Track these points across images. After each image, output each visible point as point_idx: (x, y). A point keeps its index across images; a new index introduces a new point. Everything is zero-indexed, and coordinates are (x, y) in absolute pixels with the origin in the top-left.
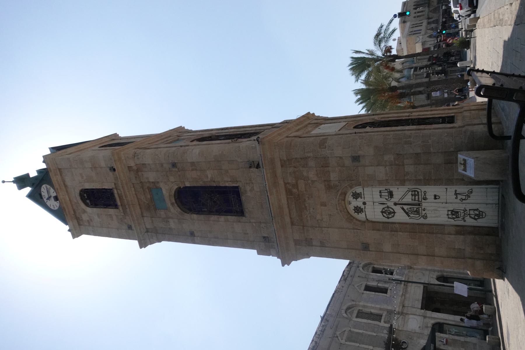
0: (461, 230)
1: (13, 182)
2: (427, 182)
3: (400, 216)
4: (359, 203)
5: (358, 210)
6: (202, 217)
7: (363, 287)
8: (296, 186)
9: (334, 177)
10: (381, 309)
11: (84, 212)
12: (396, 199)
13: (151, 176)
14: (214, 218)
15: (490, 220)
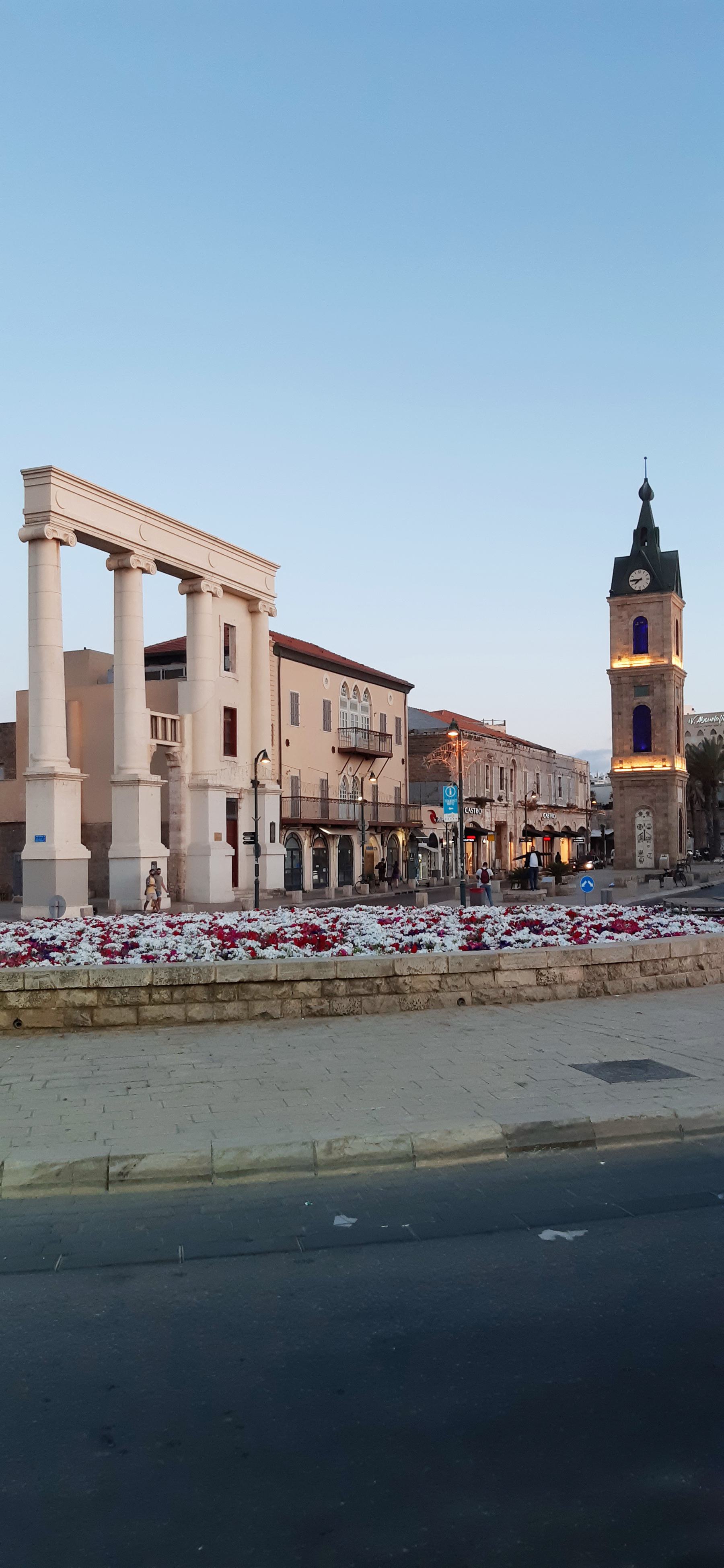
0: (634, 855)
1: (646, 480)
2: (656, 843)
3: (638, 832)
4: (644, 814)
5: (641, 814)
6: (631, 723)
7: (502, 766)
8: (653, 785)
9: (658, 804)
10: (491, 786)
11: (630, 616)
12: (647, 830)
13: (657, 690)
14: (631, 731)
15: (639, 865)
